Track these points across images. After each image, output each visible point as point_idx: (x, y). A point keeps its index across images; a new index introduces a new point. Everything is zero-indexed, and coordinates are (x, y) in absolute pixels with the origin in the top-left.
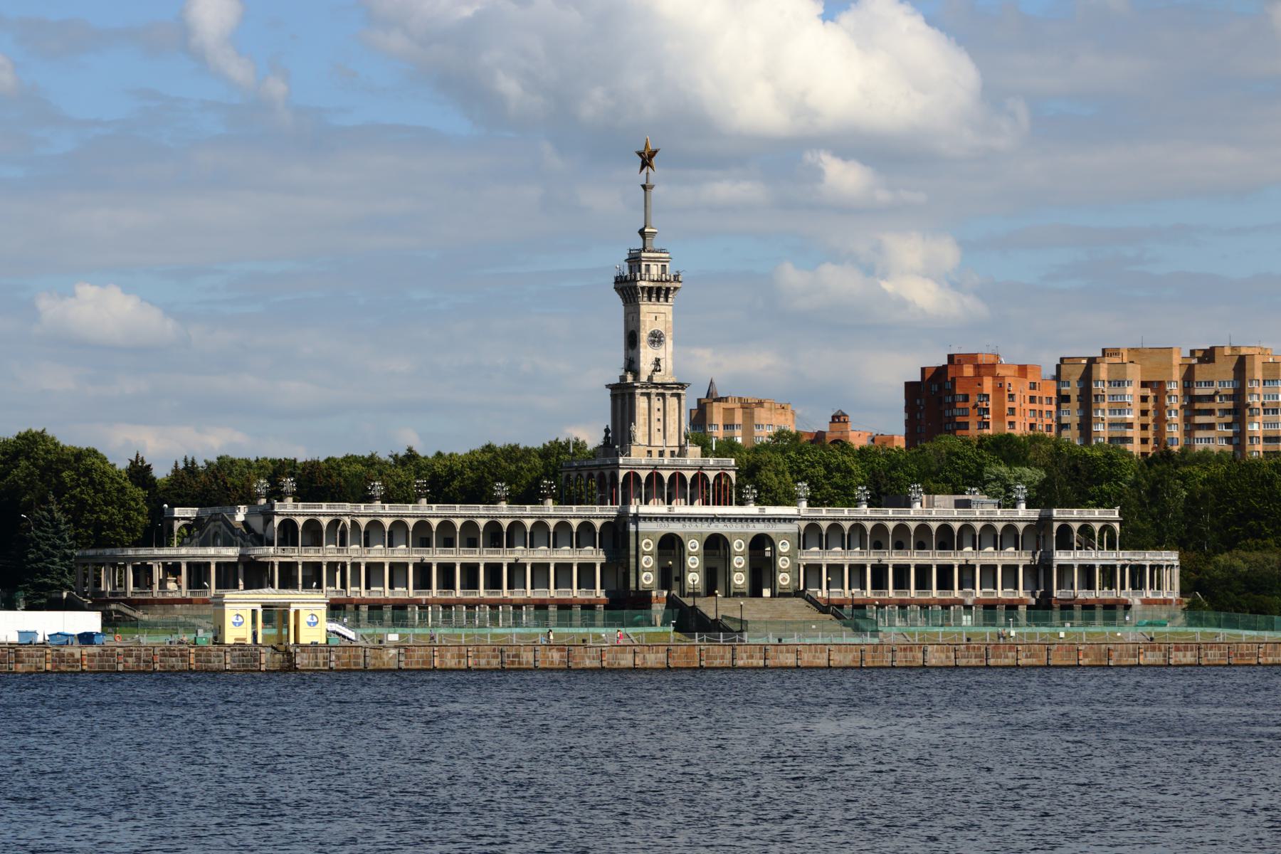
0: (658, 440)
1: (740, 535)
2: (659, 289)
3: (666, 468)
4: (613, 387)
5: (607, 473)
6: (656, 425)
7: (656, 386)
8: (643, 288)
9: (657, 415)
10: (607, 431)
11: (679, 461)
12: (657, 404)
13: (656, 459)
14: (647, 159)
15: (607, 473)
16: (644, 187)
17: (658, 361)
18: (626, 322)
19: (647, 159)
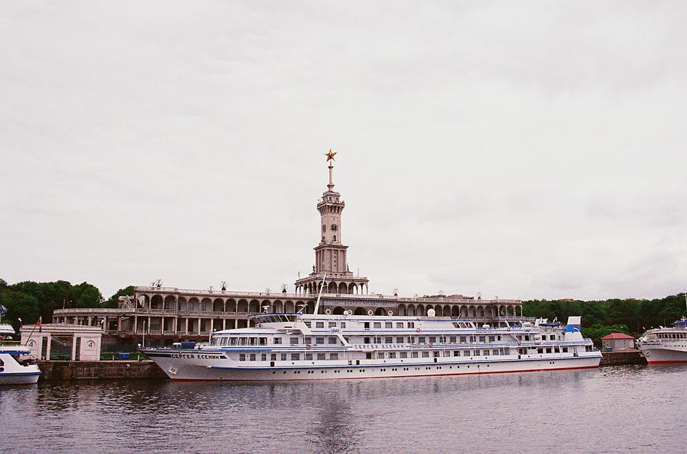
0: (334, 269)
1: (371, 308)
2: (335, 207)
3: (338, 280)
4: (316, 249)
5: (312, 283)
6: (334, 264)
7: (334, 246)
8: (328, 206)
9: (333, 259)
10: (314, 267)
11: (344, 277)
12: (334, 255)
13: (334, 277)
14: (330, 157)
15: (312, 283)
16: (329, 167)
17: (335, 236)
18: (322, 222)
19: (330, 157)
